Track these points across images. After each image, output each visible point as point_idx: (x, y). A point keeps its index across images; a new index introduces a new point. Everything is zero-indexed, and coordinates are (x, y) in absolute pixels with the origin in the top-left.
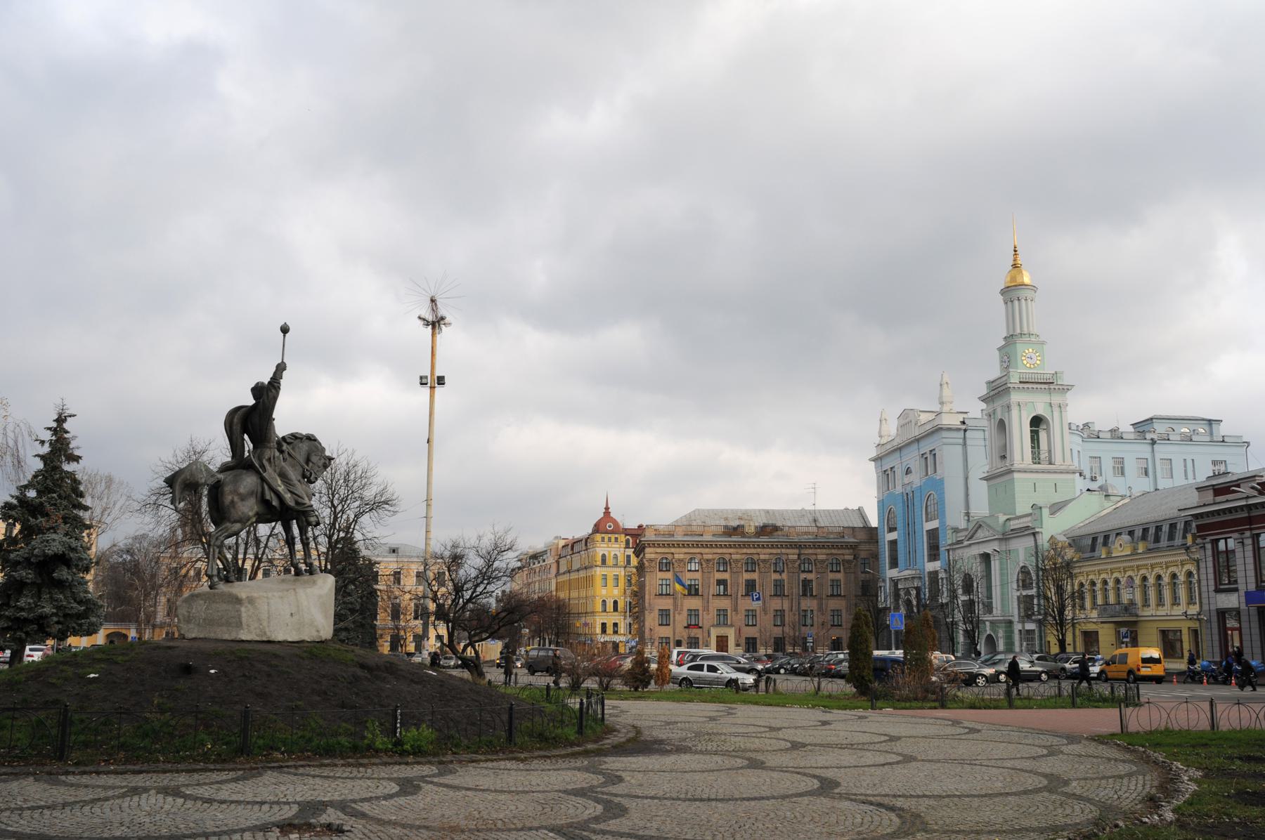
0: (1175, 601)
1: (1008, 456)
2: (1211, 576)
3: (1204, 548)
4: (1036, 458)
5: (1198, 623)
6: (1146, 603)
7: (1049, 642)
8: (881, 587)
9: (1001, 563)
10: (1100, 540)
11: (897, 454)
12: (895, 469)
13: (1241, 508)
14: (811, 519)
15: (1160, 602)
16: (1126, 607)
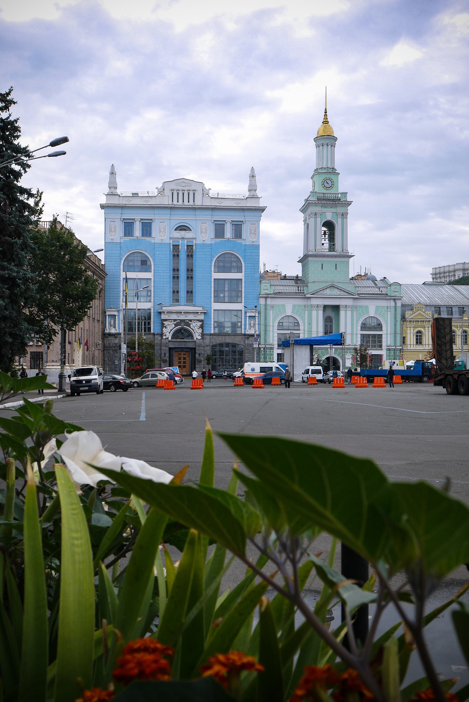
11: (168, 211)
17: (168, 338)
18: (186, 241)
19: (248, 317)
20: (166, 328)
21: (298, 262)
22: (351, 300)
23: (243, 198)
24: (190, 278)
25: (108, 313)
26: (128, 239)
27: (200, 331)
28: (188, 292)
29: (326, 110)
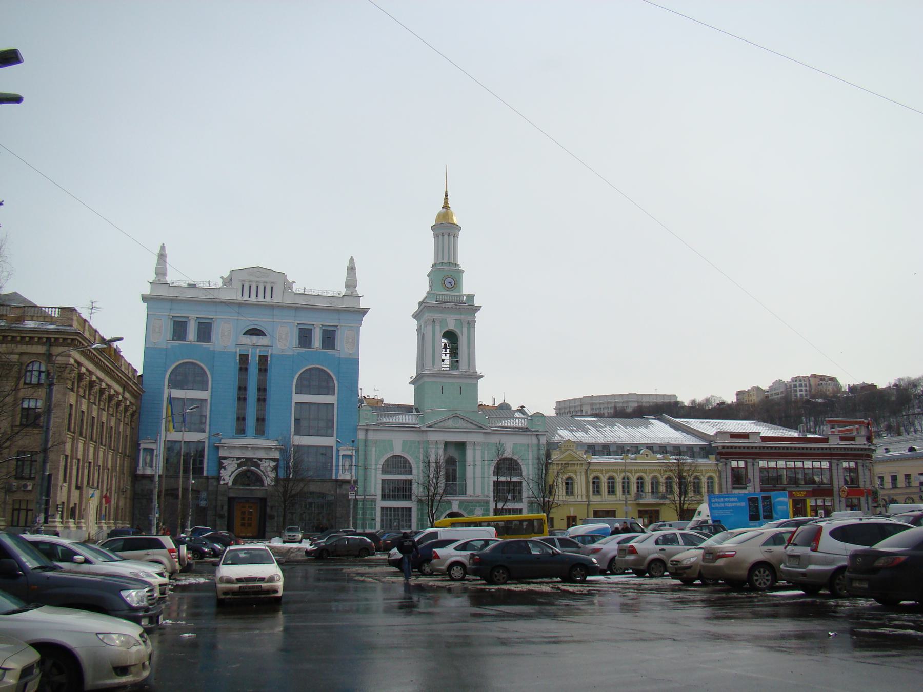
17: (227, 484)
18: (258, 350)
19: (341, 457)
20: (225, 468)
21: (410, 383)
22: (481, 436)
23: (338, 295)
24: (262, 400)
25: (142, 446)
26: (178, 345)
27: (273, 475)
28: (258, 420)
29: (446, 193)
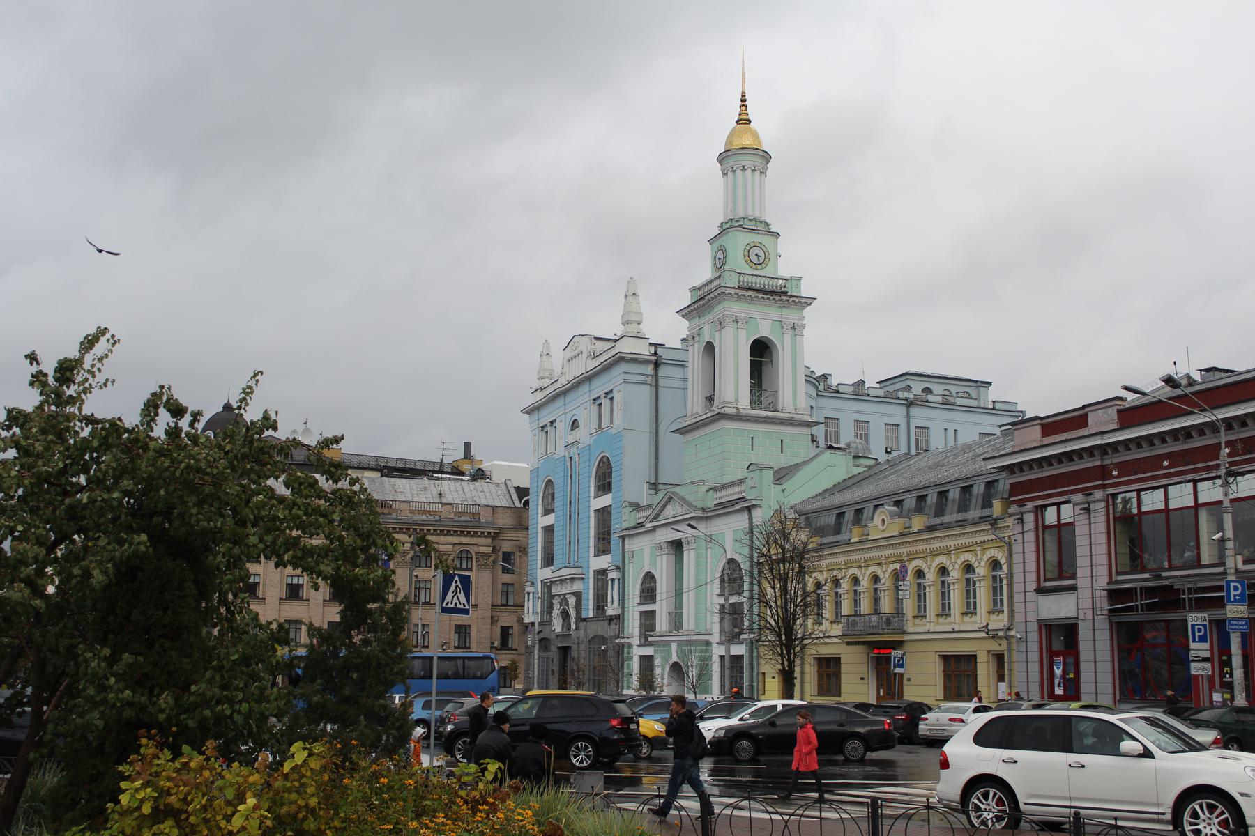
0: (970, 608)
1: (716, 398)
2: (1031, 567)
3: (1021, 520)
4: (756, 402)
5: (1004, 642)
6: (921, 614)
7: (764, 673)
8: (529, 594)
9: (697, 556)
10: (849, 516)
11: (560, 402)
12: (557, 424)
13: (1090, 451)
14: (435, 493)
15: (945, 610)
16: (888, 619)
